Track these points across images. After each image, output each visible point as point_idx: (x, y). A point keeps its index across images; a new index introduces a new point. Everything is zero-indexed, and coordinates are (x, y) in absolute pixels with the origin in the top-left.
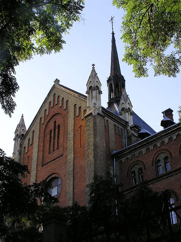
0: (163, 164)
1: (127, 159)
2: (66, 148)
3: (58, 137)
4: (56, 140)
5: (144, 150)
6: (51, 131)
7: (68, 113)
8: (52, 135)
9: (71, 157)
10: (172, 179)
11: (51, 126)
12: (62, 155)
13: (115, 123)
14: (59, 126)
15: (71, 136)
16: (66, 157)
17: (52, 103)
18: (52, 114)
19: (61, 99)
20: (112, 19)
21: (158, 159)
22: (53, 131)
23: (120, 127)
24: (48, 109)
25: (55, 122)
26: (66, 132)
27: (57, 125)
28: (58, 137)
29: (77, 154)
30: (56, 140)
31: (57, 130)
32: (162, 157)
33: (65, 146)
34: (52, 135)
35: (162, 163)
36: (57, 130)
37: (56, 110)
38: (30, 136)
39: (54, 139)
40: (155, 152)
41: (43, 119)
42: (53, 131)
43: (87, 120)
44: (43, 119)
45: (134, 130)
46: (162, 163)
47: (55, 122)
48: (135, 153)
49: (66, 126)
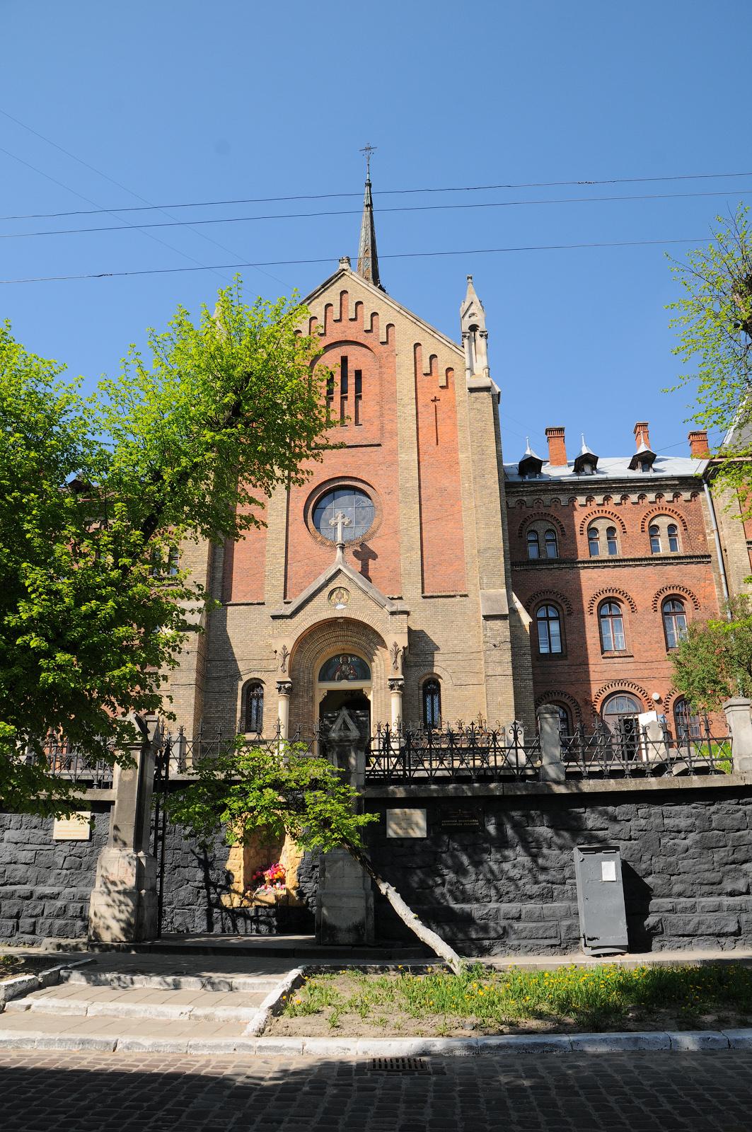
1: (521, 502)
2: (394, 434)
3: (358, 397)
9: (408, 457)
12: (379, 445)
14: (358, 374)
16: (394, 452)
18: (335, 334)
25: (344, 360)
26: (388, 398)
27: (352, 367)
28: (358, 397)
29: (426, 457)
31: (351, 381)
33: (388, 427)
36: (351, 381)
37: (352, 332)
39: (344, 398)
42: (337, 378)
43: (477, 398)
47: (344, 360)
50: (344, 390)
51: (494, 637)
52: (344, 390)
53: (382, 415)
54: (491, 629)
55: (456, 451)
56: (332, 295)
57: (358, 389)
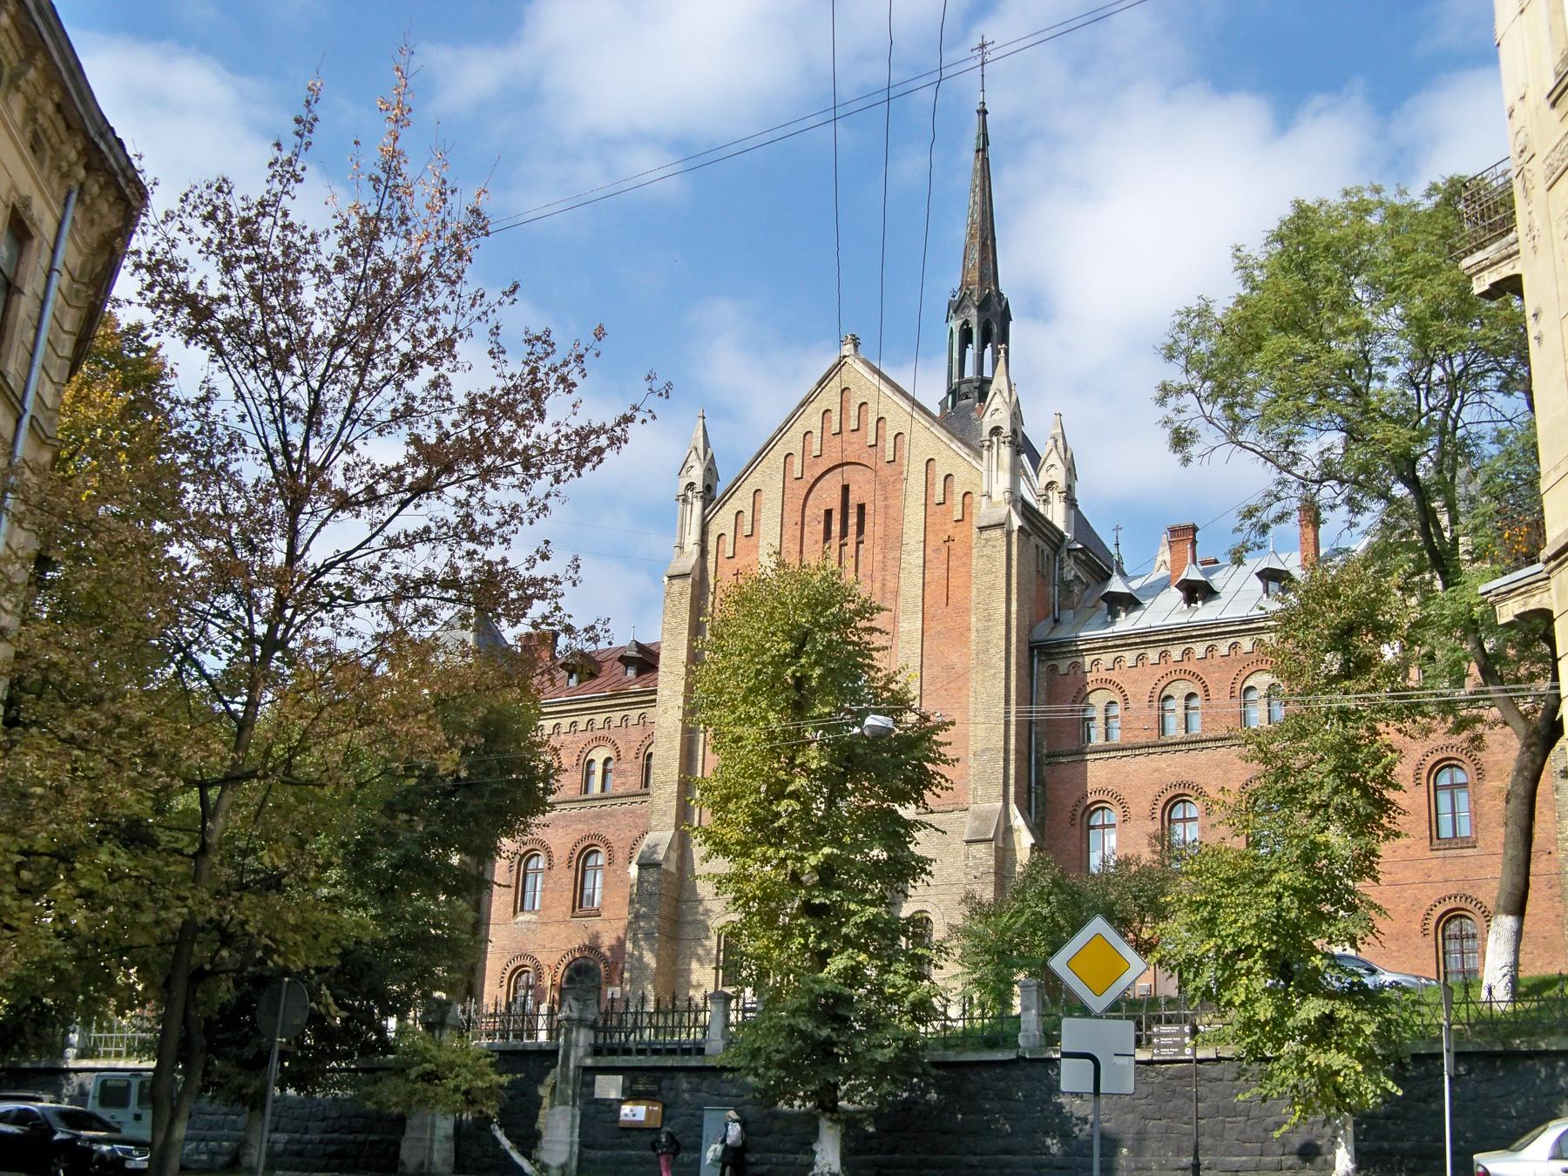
0: (1180, 711)
4: (850, 549)
5: (1129, 656)
6: (828, 513)
7: (901, 478)
8: (836, 528)
9: (910, 625)
10: (1200, 757)
11: (828, 494)
13: (1041, 543)
14: (861, 508)
15: (913, 559)
17: (835, 416)
19: (872, 419)
20: (983, 46)
21: (1166, 693)
22: (836, 516)
23: (1047, 550)
24: (817, 433)
25: (846, 489)
26: (894, 541)
27: (854, 500)
30: (850, 549)
31: (853, 520)
32: (1179, 690)
33: (891, 585)
34: (836, 528)
35: (1177, 704)
36: (853, 520)
38: (742, 500)
40: (1160, 671)
41: (797, 461)
42: (836, 516)
43: (987, 540)
44: (797, 461)
45: (1076, 558)
46: (1177, 704)
47: (846, 489)
48: (1103, 657)
49: (895, 520)
50: (844, 533)
51: (976, 867)
52: (844, 533)
53: (884, 569)
54: (974, 857)
55: (967, 611)
56: (830, 398)
57: (860, 531)
